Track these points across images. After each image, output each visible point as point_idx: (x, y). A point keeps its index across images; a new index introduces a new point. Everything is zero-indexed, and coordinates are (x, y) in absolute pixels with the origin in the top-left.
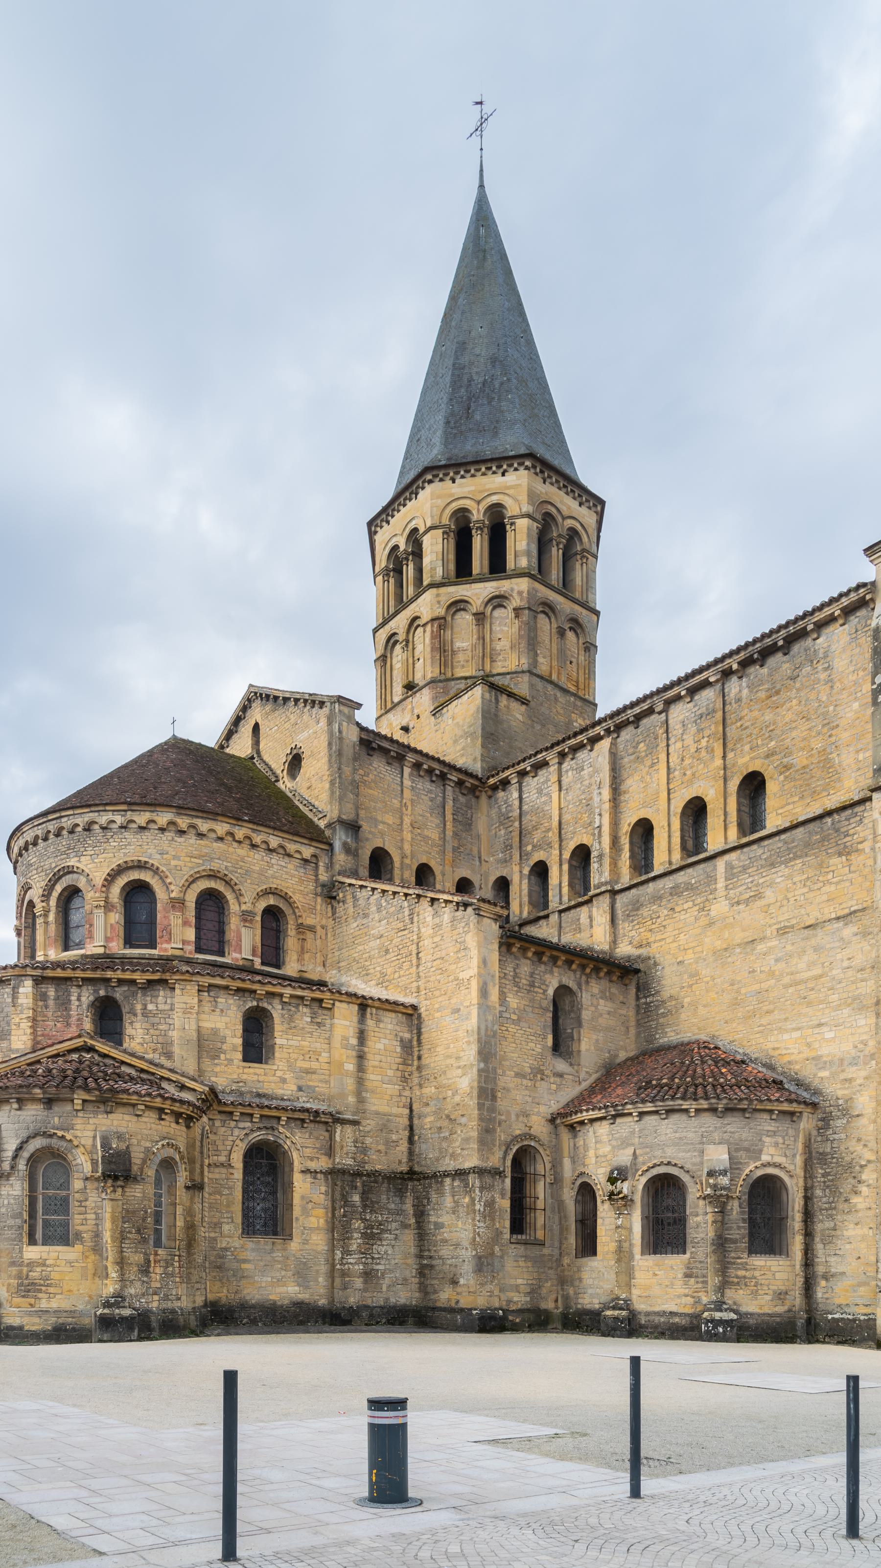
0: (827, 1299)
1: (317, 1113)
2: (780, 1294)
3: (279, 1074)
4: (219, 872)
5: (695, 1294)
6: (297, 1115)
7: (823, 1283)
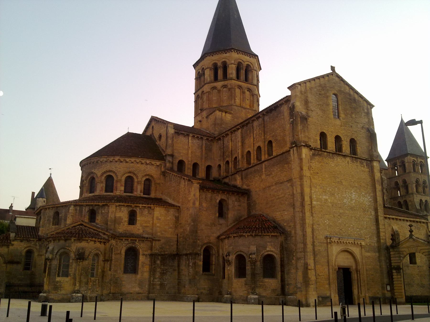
0: (288, 291)
1: (147, 238)
2: (274, 290)
3: (137, 228)
4: (131, 171)
5: (248, 290)
6: (141, 239)
7: (287, 287)
